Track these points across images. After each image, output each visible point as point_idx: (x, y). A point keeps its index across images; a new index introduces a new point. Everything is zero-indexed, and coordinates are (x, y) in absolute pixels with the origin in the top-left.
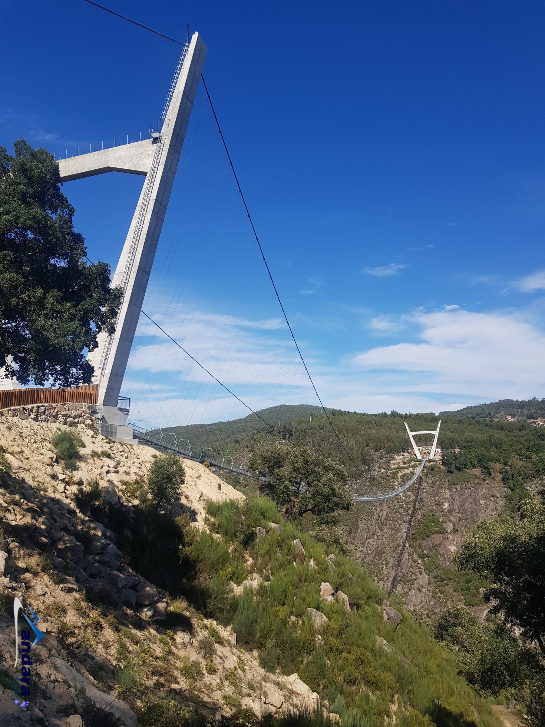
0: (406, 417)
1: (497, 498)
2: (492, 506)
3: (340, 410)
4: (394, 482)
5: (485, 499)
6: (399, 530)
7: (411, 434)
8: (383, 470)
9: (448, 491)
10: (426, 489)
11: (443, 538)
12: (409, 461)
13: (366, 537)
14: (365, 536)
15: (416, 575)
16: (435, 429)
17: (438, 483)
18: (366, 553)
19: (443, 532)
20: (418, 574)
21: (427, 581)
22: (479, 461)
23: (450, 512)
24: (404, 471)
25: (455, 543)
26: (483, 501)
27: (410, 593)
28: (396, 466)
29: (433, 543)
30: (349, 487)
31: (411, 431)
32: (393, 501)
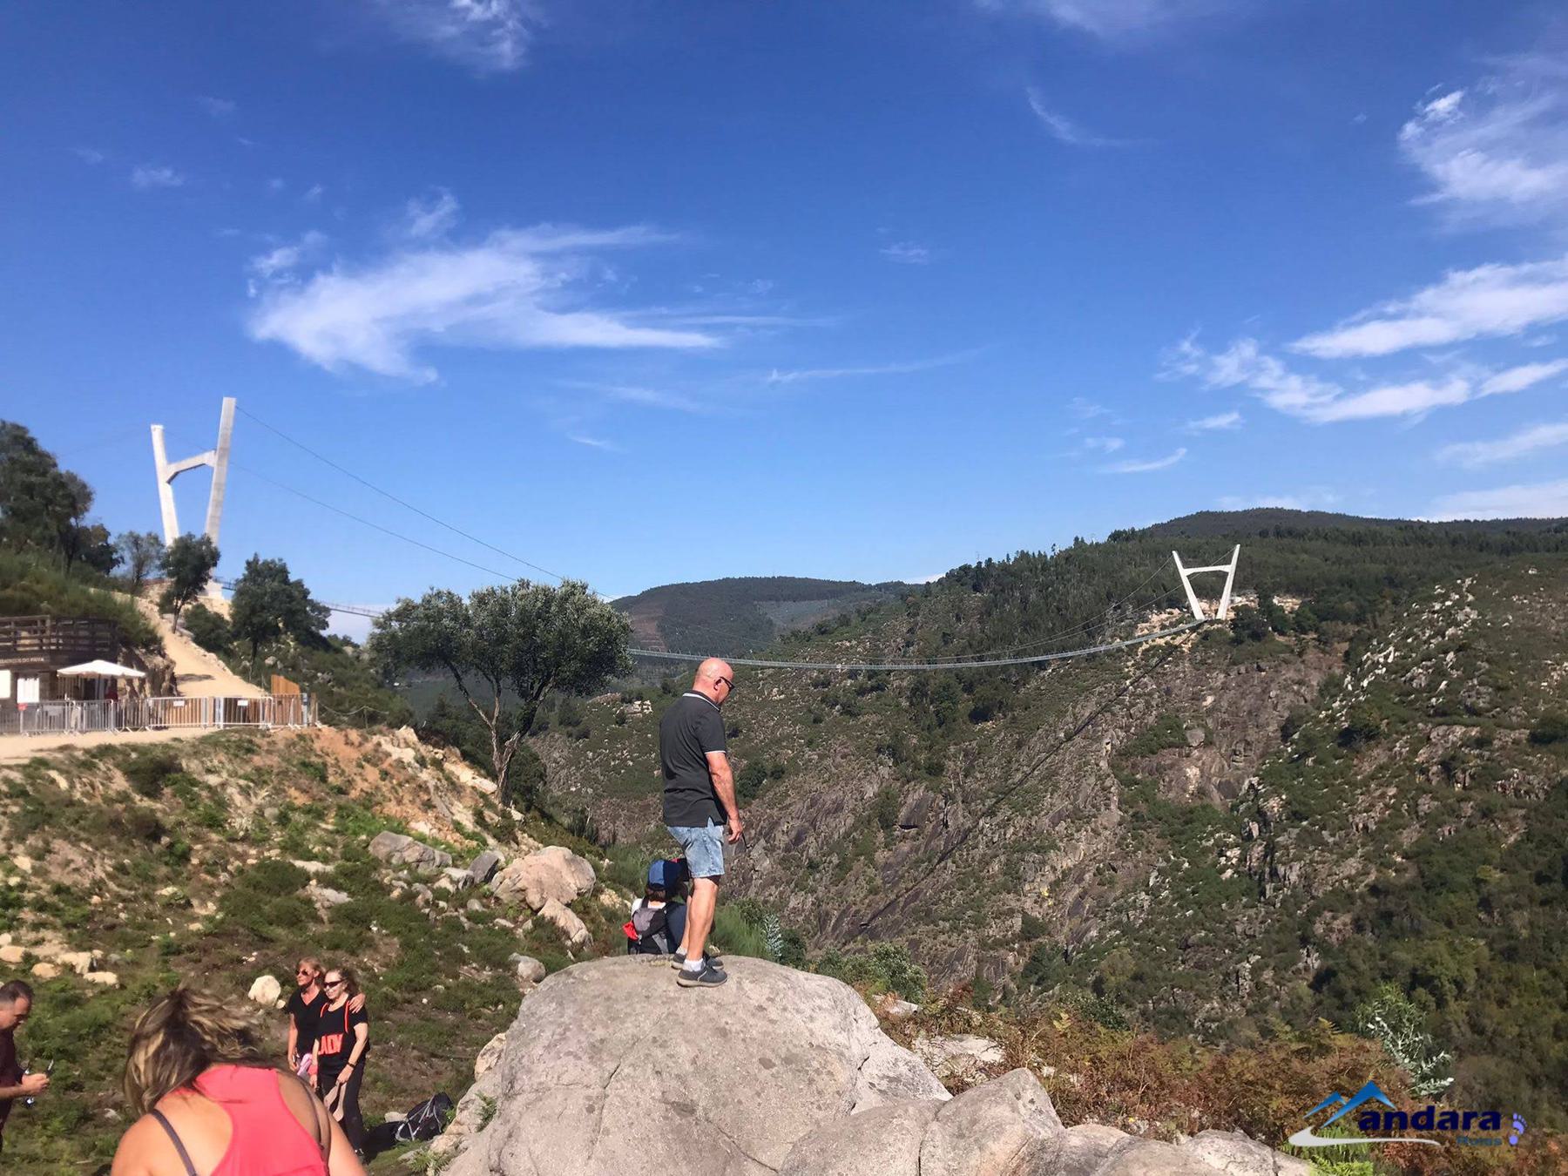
6: (1099, 740)
7: (1184, 573)
10: (1184, 672)
11: (1180, 754)
15: (1099, 810)
17: (1210, 661)
20: (1103, 808)
21: (1116, 819)
23: (1211, 711)
25: (1200, 763)
27: (1076, 836)
29: (1159, 763)
31: (1186, 565)
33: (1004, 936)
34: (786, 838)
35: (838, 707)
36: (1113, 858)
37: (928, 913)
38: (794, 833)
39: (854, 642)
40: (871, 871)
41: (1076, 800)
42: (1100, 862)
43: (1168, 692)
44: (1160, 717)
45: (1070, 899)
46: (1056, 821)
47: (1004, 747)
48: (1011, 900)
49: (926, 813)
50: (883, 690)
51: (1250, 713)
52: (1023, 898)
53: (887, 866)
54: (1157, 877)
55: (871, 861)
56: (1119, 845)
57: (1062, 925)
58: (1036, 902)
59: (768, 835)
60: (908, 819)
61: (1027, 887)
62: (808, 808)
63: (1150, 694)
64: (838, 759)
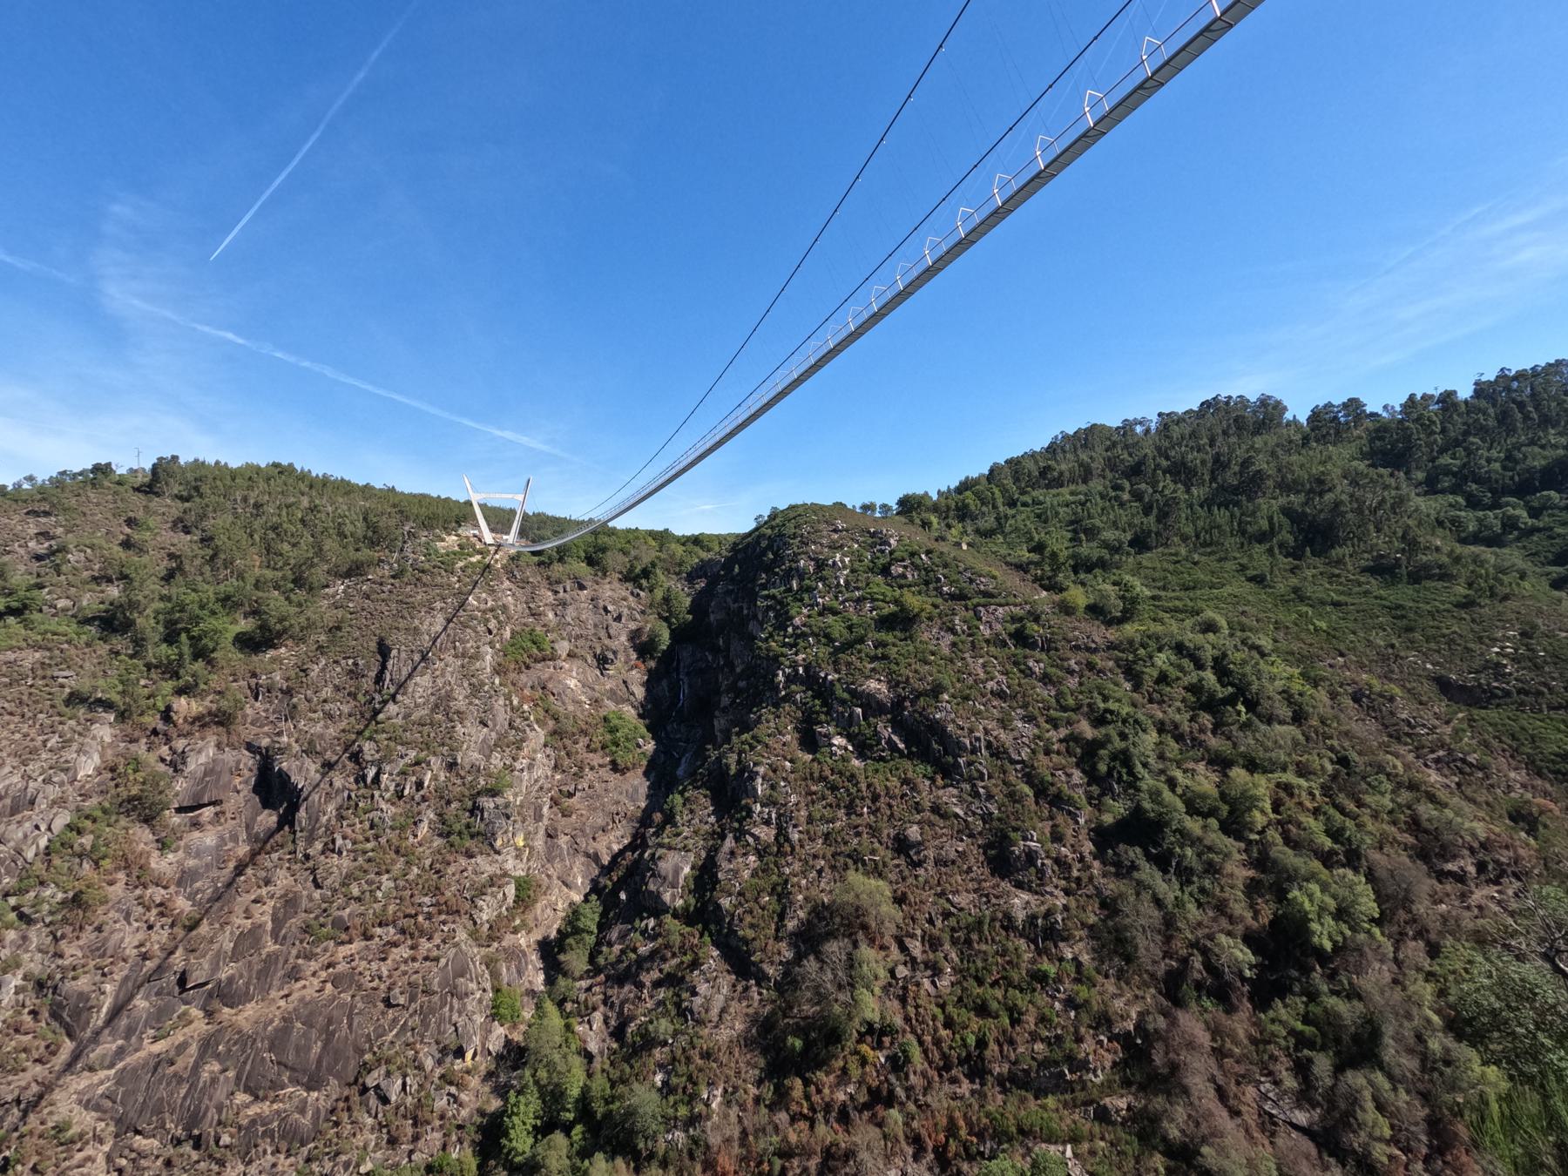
6: (477, 656)
9: (550, 593)
19: (554, 658)
21: (542, 740)
27: (518, 766)
33: (499, 916)
36: (562, 783)
37: (341, 925)
41: (495, 726)
42: (550, 790)
43: (505, 608)
44: (513, 632)
45: (539, 842)
46: (487, 752)
48: (485, 865)
49: (230, 782)
51: (596, 626)
52: (497, 857)
53: (185, 878)
55: (141, 877)
56: (556, 767)
57: (548, 876)
58: (517, 857)
61: (499, 843)
63: (492, 610)
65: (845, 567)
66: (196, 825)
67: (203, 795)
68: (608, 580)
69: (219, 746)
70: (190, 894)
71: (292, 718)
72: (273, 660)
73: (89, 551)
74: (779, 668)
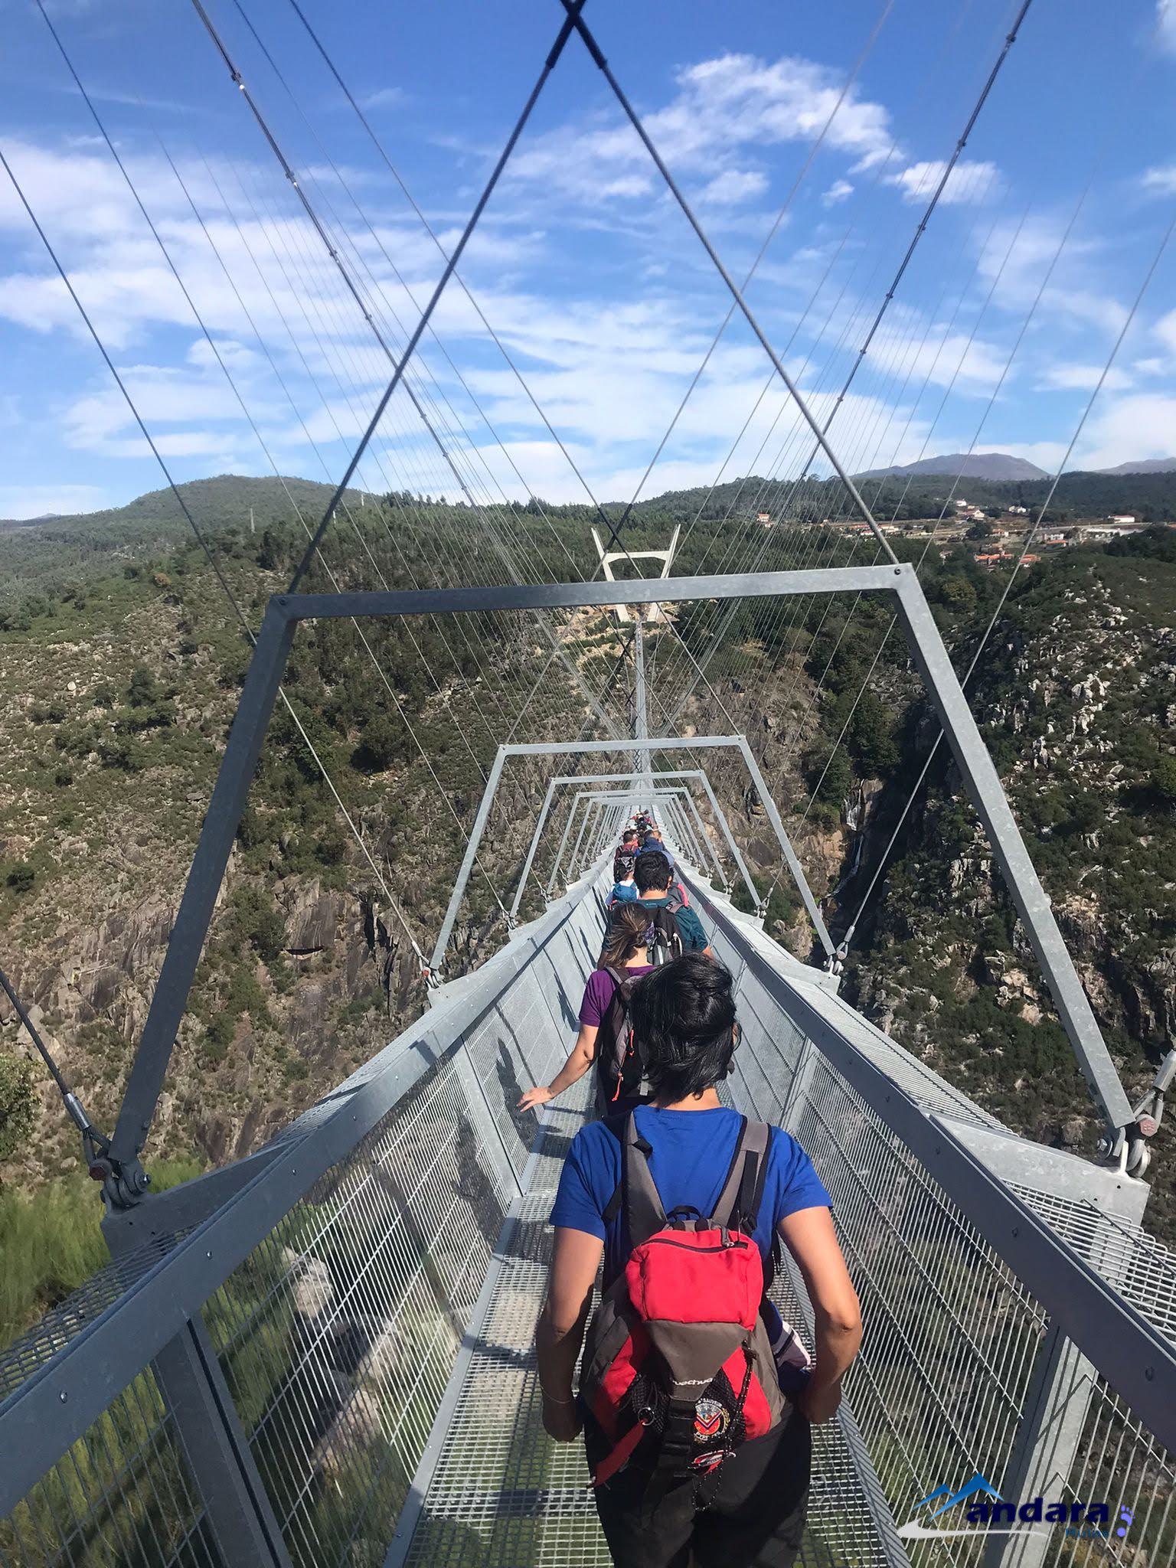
0: (599, 516)
1: (804, 710)
2: (793, 729)
3: (407, 494)
4: (569, 679)
5: (777, 716)
8: (539, 651)
9: (693, 698)
12: (602, 627)
13: (508, 816)
14: (504, 816)
16: (667, 549)
17: (670, 678)
18: (509, 856)
22: (758, 625)
24: (589, 651)
25: (712, 821)
26: (774, 721)
28: (570, 639)
30: (455, 692)
31: (609, 548)
32: (568, 727)
34: (75, 995)
35: (92, 756)
38: (90, 987)
39: (86, 646)
40: (273, 1038)
47: (431, 812)
49: (335, 927)
50: (169, 724)
53: (296, 1024)
54: (892, 1023)
59: (44, 998)
60: (305, 940)
62: (107, 940)
64: (133, 847)
65: (1097, 699)
66: (305, 969)
67: (310, 941)
68: (780, 673)
69: (323, 885)
70: (299, 1042)
71: (391, 862)
72: (379, 787)
73: (211, 649)
74: (959, 857)
